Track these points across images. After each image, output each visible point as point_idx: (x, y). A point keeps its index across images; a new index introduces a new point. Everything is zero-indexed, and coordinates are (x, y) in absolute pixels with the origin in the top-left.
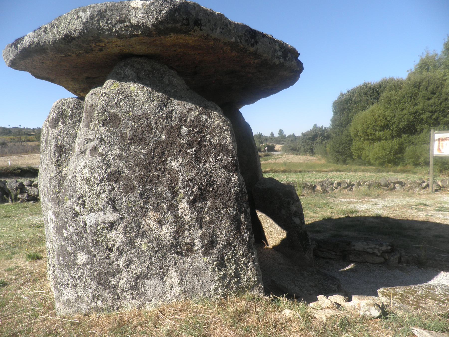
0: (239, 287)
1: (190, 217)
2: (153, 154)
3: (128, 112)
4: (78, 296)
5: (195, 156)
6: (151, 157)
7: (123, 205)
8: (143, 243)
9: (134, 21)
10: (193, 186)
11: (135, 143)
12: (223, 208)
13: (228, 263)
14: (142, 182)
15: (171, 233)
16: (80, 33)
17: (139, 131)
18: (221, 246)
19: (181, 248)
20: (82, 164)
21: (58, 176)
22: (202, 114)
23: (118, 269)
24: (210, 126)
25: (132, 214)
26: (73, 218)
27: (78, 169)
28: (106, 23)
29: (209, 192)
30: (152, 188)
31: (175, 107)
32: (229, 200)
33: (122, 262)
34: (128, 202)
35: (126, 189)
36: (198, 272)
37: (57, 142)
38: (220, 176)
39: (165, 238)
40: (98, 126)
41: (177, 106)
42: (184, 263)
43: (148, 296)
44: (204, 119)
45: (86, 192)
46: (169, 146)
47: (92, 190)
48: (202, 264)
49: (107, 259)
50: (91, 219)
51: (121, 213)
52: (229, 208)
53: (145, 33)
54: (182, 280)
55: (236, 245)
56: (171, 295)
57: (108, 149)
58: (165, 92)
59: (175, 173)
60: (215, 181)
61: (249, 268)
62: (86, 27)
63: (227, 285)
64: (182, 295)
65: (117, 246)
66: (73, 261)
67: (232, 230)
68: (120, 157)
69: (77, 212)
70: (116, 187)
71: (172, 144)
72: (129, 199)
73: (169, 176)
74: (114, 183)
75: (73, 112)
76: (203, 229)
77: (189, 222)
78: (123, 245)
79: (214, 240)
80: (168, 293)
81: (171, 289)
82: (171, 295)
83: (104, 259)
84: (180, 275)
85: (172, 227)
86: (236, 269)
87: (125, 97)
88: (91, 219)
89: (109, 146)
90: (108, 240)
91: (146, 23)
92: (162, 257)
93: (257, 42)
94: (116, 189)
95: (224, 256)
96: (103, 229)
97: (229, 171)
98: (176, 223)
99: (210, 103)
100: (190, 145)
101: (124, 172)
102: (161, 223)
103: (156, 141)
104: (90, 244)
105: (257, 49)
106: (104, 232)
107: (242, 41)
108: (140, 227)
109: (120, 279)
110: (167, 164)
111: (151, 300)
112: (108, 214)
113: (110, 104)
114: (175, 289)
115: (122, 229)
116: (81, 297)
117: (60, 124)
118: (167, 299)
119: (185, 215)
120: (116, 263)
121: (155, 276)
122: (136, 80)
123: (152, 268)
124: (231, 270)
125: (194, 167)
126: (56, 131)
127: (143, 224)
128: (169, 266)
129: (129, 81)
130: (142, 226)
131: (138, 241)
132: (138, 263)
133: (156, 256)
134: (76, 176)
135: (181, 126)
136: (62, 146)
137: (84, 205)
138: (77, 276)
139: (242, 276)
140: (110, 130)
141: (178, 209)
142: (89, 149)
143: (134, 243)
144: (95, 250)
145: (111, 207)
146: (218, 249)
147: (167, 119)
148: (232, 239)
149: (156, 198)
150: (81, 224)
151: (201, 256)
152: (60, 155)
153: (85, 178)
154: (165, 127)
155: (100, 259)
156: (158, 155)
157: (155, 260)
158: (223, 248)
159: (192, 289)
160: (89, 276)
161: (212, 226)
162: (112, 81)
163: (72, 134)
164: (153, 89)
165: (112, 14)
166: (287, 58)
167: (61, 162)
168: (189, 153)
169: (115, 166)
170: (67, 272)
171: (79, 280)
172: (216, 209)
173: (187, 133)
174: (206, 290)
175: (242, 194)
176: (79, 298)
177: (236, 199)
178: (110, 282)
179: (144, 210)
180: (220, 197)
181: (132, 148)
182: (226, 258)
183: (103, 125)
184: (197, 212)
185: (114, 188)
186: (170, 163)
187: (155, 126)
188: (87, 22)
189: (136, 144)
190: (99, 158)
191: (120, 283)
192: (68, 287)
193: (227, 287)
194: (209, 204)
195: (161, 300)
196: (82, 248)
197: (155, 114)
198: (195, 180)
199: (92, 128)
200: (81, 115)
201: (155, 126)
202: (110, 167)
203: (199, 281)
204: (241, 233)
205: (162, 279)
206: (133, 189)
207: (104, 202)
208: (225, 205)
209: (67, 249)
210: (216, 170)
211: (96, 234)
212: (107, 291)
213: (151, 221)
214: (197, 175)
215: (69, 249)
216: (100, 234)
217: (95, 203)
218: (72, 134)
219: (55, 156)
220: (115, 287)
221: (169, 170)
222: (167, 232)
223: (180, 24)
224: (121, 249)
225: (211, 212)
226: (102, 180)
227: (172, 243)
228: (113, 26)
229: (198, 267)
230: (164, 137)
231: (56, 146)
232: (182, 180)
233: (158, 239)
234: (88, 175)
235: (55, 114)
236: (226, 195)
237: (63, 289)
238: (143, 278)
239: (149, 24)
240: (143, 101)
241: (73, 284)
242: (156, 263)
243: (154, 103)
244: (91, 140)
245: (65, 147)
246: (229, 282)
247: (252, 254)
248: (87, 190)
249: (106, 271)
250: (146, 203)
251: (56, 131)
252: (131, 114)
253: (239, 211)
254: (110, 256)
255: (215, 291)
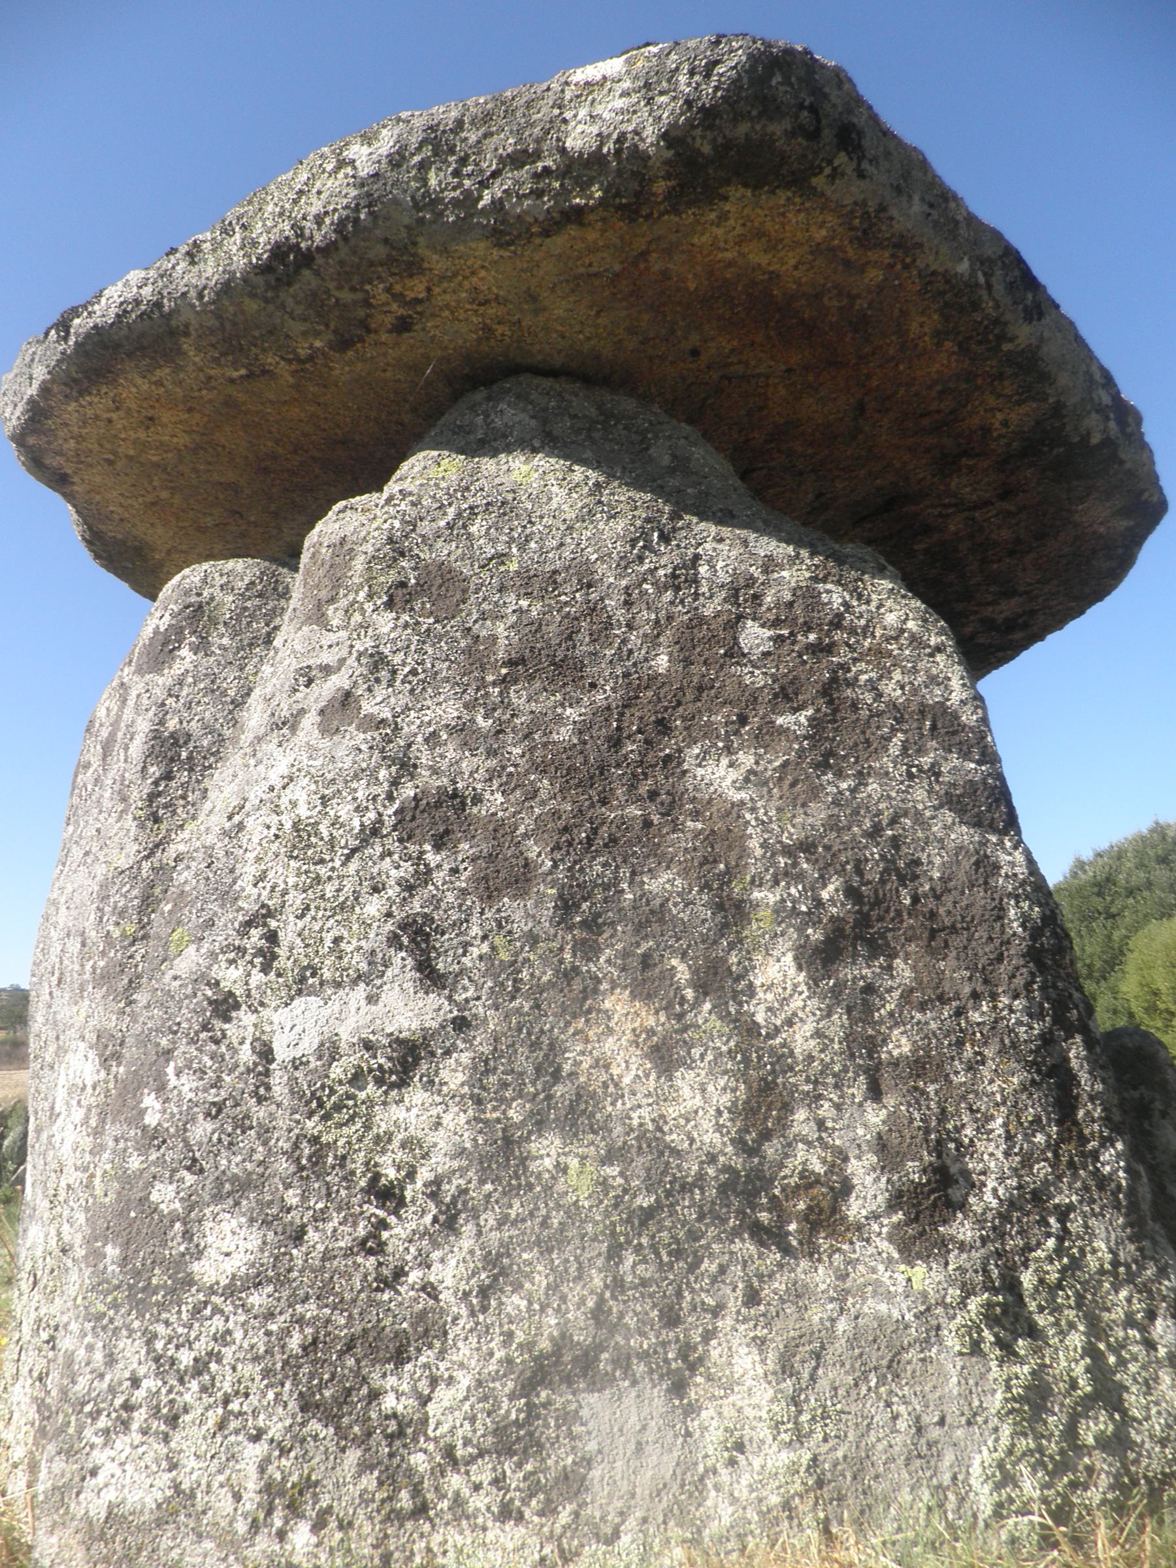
1: (818, 1034)
2: (619, 728)
3: (502, 558)
4: (176, 1486)
5: (813, 747)
6: (609, 739)
7: (469, 952)
8: (574, 1163)
9: (579, 137)
10: (822, 877)
11: (531, 678)
12: (976, 996)
13: (1041, 1309)
14: (570, 844)
15: (719, 1113)
16: (340, 227)
17: (551, 631)
18: (994, 1203)
19: (775, 1205)
20: (282, 768)
21: (146, 866)
22: (824, 580)
23: (424, 1312)
24: (865, 628)
25: (516, 1003)
26: (205, 1027)
27: (256, 793)
28: (456, 173)
29: (899, 913)
30: (616, 880)
31: (707, 546)
32: (1000, 959)
33: (451, 1270)
34: (498, 941)
35: (486, 878)
36: (887, 1358)
37: (162, 722)
38: (941, 841)
39: (692, 1141)
40: (369, 607)
41: (715, 545)
42: (799, 1294)
43: (601, 1500)
44: (837, 600)
45: (285, 893)
46: (689, 696)
47: (318, 879)
48: (902, 1310)
49: (371, 1252)
50: (297, 1028)
51: (460, 997)
52: (1005, 1000)
53: (618, 194)
54: (795, 1401)
55: (1070, 1208)
56: (734, 1500)
57: (404, 699)
58: (659, 491)
59: (728, 813)
60: (917, 862)
61: (1162, 1352)
62: (369, 195)
63: (1062, 1452)
64: (803, 1507)
65: (430, 1176)
66: (180, 1262)
67: (1037, 1120)
68: (462, 730)
69: (231, 994)
70: (439, 866)
71: (700, 689)
72: (500, 926)
73: (699, 826)
74: (427, 847)
75: (246, 609)
76: (890, 1101)
77: (810, 1058)
78: (463, 1171)
79: (954, 1169)
80: (717, 1488)
81: (732, 1462)
82: (734, 1500)
83: (349, 1252)
84: (786, 1368)
85: (722, 1082)
87: (488, 504)
88: (297, 1028)
89: (412, 691)
90: (382, 1142)
91: (636, 132)
92: (677, 1254)
94: (439, 877)
95: (1014, 1268)
96: (357, 1078)
97: (977, 823)
98: (746, 1060)
99: (849, 549)
100: (787, 695)
101: (477, 799)
102: (665, 1056)
103: (626, 675)
104: (283, 1166)
106: (362, 1095)
107: (994, 280)
108: (559, 1069)
109: (434, 1382)
110: (685, 772)
111: (616, 1534)
112: (391, 996)
113: (425, 528)
114: (757, 1463)
115: (461, 1077)
116: (192, 1496)
117: (185, 652)
118: (713, 1528)
119: (789, 1022)
120: (414, 1276)
121: (640, 1368)
122: (537, 443)
123: (621, 1316)
124: (1068, 1357)
125: (815, 792)
126: (164, 680)
127: (573, 1056)
128: (717, 1311)
129: (509, 450)
130: (567, 1068)
131: (546, 1150)
132: (541, 1280)
133: (645, 1241)
134: (241, 827)
135: (740, 617)
136: (178, 740)
137: (268, 958)
138: (186, 1358)
139: (1134, 1401)
140: (417, 623)
141: (751, 990)
142: (315, 708)
143: (523, 1161)
144: (304, 1198)
145: (410, 962)
146: (980, 1221)
147: (677, 589)
148: (1042, 1169)
149: (640, 927)
150: (246, 1055)
151: (890, 1260)
152: (168, 776)
153: (288, 825)
154: (670, 618)
155: (327, 1256)
156: (639, 731)
157: (641, 1268)
158: (1005, 1217)
159: (860, 1465)
160: (256, 1359)
161: (931, 1089)
162: (435, 453)
163: (231, 693)
164: (611, 476)
165: (485, 136)
167: (166, 806)
168: (783, 731)
169: (435, 771)
170: (131, 1332)
171: (194, 1385)
172: (942, 999)
173: (769, 646)
174: (946, 1479)
176: (180, 1503)
178: (375, 1395)
179: (577, 985)
180: (957, 941)
181: (518, 697)
182: (1027, 1279)
183: (390, 605)
184: (849, 1011)
185: (429, 871)
186: (700, 772)
187: (620, 614)
188: (376, 175)
189: (537, 685)
190: (362, 736)
191: (431, 1408)
192: (126, 1424)
193: (1062, 1466)
194: (904, 971)
195: (675, 1532)
196: (232, 1190)
197: (624, 564)
198: (827, 848)
199: (335, 622)
200: (277, 621)
201: (620, 614)
202: (412, 777)
203: (895, 1418)
204: (1083, 1140)
205: (679, 1387)
206: (521, 879)
207: (376, 939)
208: (986, 982)
209: (154, 1197)
210: (918, 814)
211: (321, 1105)
212: (353, 1456)
213: (614, 1041)
214: (832, 825)
215: (165, 1196)
216: (338, 1107)
217: (328, 943)
218: (231, 693)
219: (144, 778)
220: (404, 1431)
221: (693, 800)
222: (699, 1107)
223: (787, 124)
224: (449, 1190)
225: (918, 1016)
226: (374, 831)
227: (727, 1169)
228: (484, 185)
229: (881, 1321)
230: (662, 662)
231: (156, 735)
232: (764, 845)
233: (653, 1142)
234: (303, 811)
235: (167, 617)
236: (981, 933)
237: (99, 1441)
238: (568, 1380)
239: (650, 133)
240: (570, 515)
241: (158, 1408)
242: (644, 1283)
243: (620, 525)
244: (327, 670)
245: (191, 745)
246: (1071, 1432)
248: (291, 881)
249: (357, 1329)
250: (589, 950)
251: (164, 680)
252: (514, 567)
253: (1055, 1021)
254: (385, 1235)
255: (998, 1487)
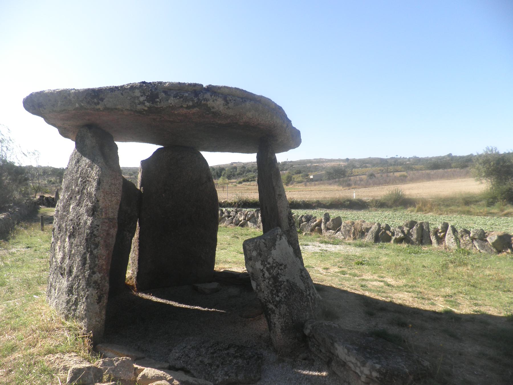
0: (74, 314)
86: (76, 299)
93: (102, 99)
105: (105, 105)
139: (79, 306)
166: (157, 100)
175: (91, 236)
177: (86, 240)
204: (84, 270)
247: (88, 291)
